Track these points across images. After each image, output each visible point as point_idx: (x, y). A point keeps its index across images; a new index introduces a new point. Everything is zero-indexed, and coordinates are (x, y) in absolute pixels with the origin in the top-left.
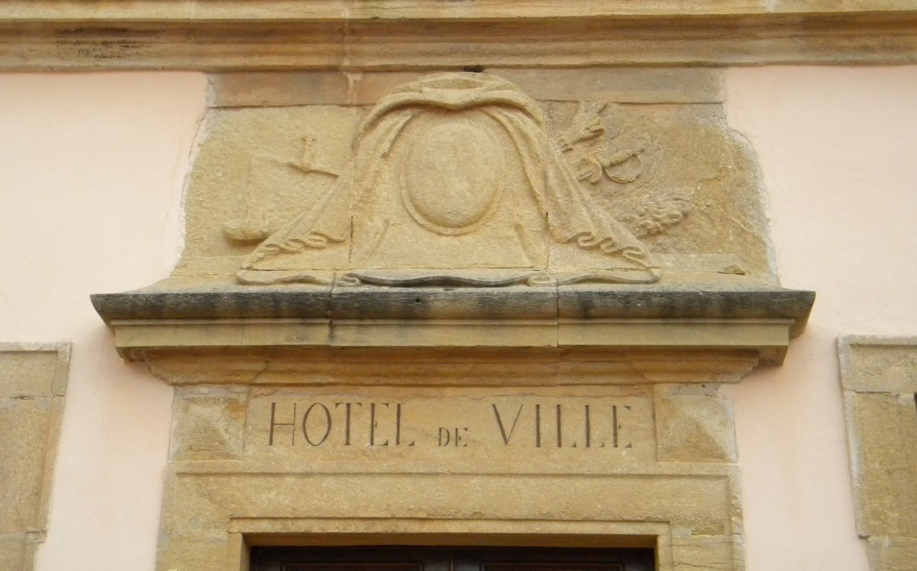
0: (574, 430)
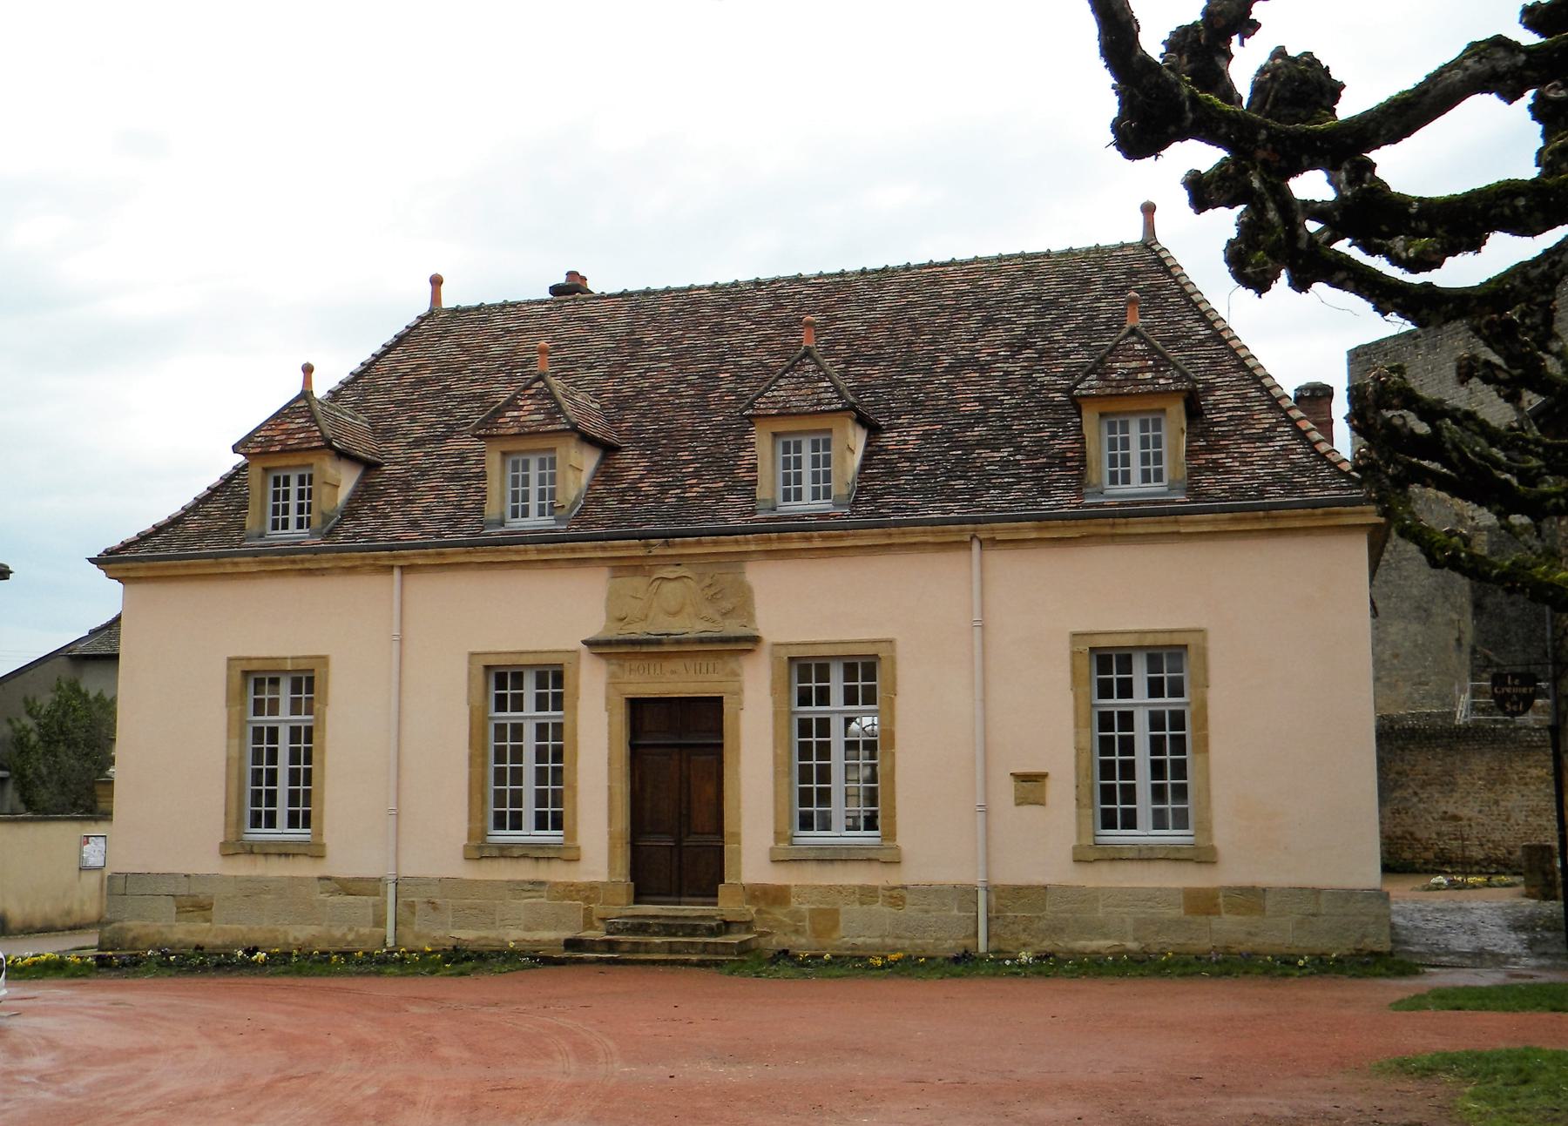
0: (704, 670)
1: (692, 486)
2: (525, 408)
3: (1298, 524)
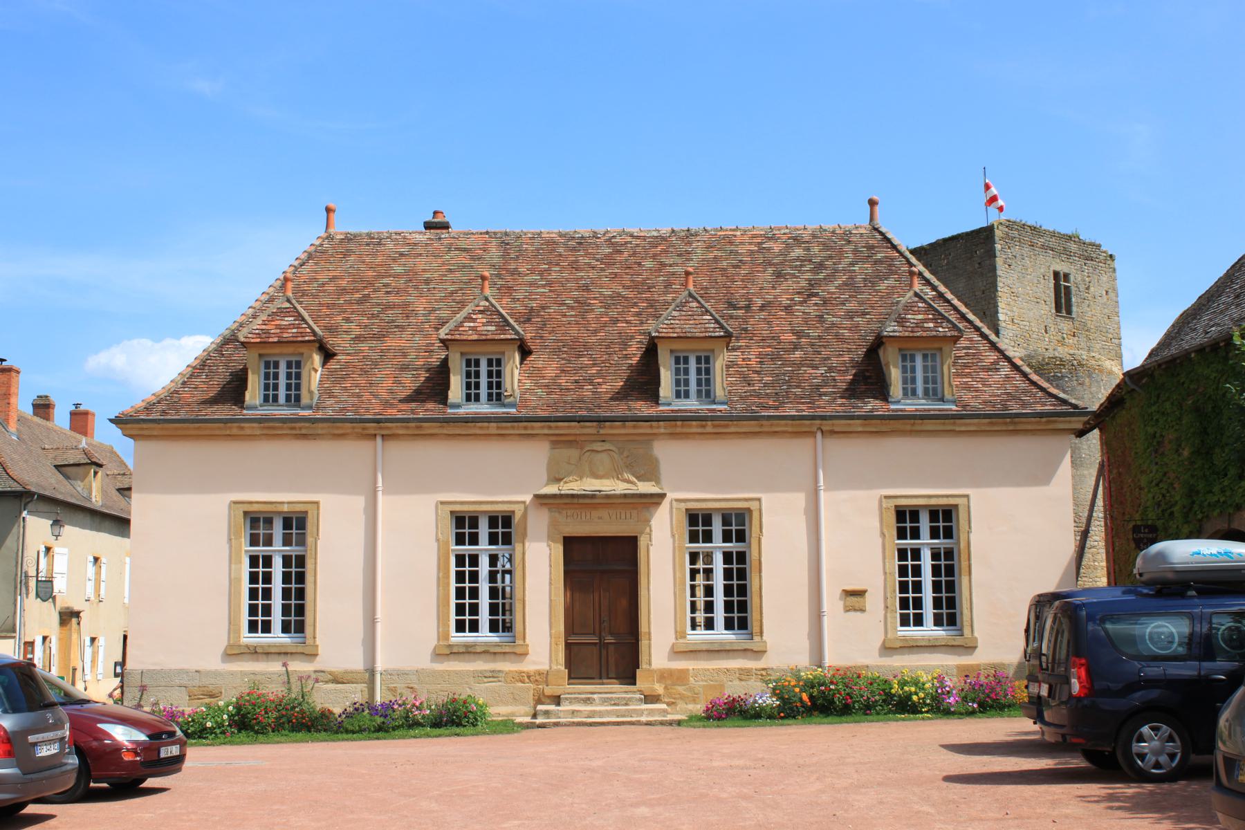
0: (623, 517)
1: (599, 384)
2: (478, 320)
3: (1029, 427)
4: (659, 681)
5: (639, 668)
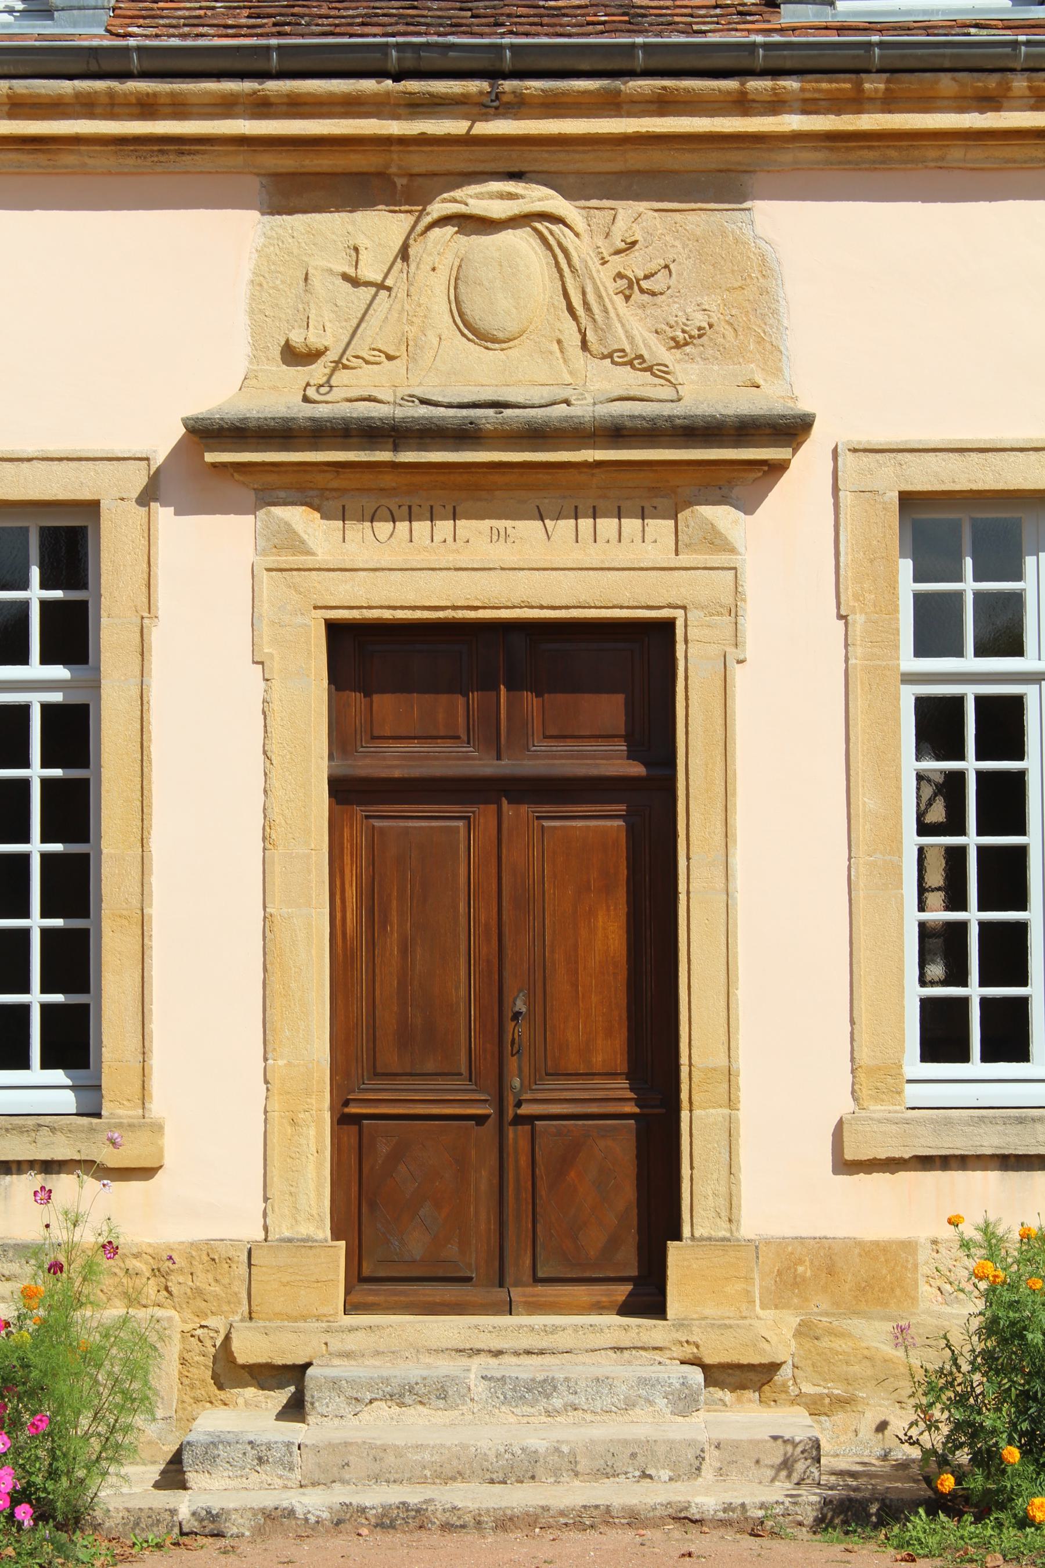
4: (776, 1300)
5: (678, 1237)
